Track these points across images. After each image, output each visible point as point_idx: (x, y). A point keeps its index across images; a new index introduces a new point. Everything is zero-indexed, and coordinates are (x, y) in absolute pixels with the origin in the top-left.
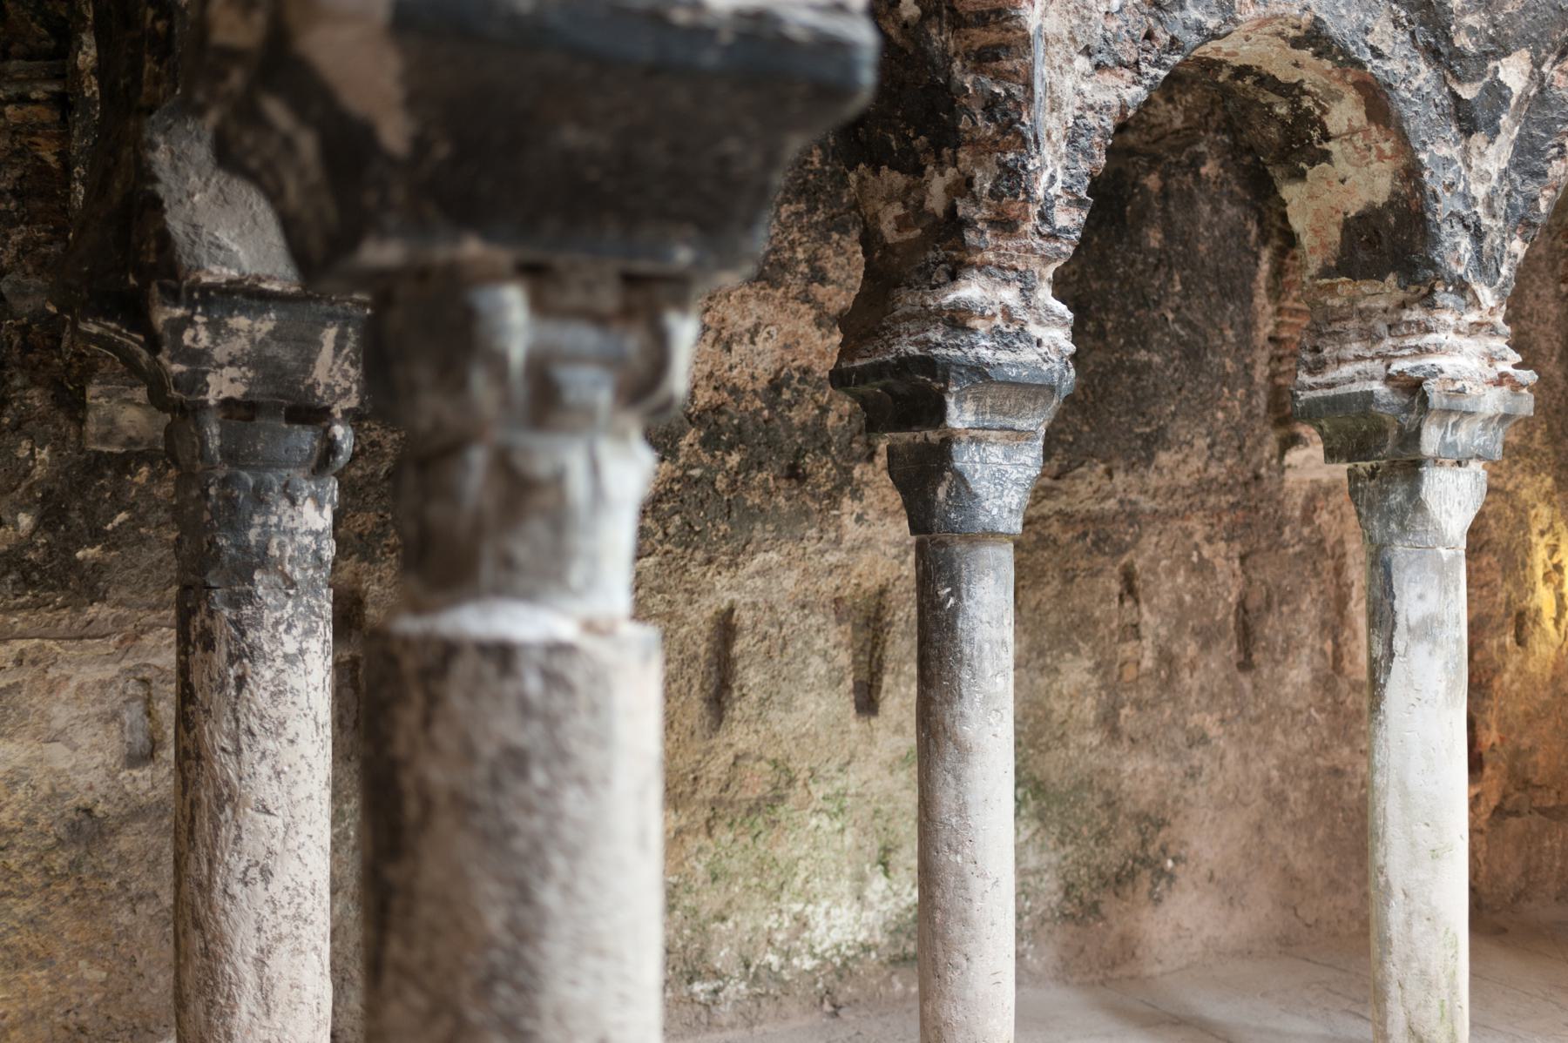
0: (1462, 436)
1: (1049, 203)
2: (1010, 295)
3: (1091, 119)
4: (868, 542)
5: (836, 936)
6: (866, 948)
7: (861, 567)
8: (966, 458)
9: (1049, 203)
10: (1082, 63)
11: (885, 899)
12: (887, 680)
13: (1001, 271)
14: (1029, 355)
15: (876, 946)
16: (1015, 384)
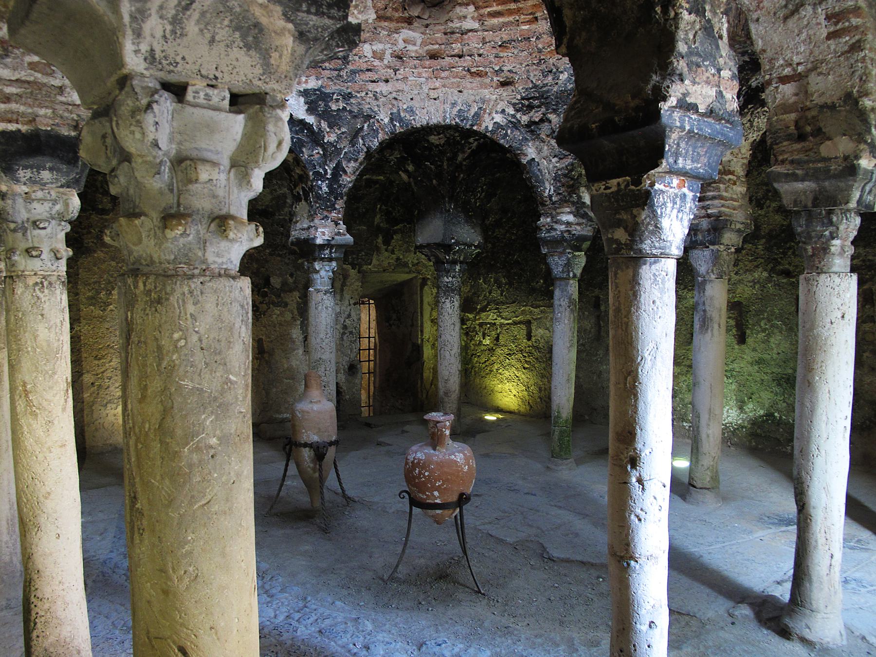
0: (700, 237)
1: (550, 196)
2: (549, 220)
3: (560, 173)
4: (740, 281)
5: (730, 419)
6: (743, 427)
7: (738, 291)
8: (550, 260)
9: (550, 196)
10: (554, 160)
11: (751, 412)
12: (748, 332)
13: (546, 215)
14: (553, 233)
15: (746, 427)
16: (549, 241)
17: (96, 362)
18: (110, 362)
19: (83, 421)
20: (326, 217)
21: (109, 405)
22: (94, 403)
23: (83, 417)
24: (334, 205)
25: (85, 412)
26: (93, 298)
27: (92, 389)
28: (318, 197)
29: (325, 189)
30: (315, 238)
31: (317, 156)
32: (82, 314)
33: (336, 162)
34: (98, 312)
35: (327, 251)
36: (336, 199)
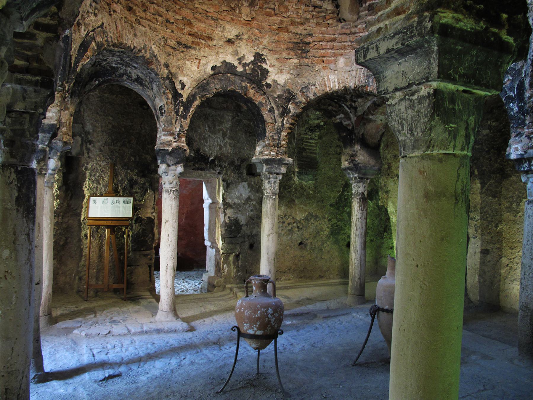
17: (511, 251)
18: (519, 252)
19: (500, 288)
20: (519, 135)
21: (515, 282)
22: (506, 278)
23: (500, 285)
24: (524, 120)
25: (501, 283)
26: (509, 207)
27: (506, 268)
28: (513, 118)
29: (516, 109)
30: (510, 154)
31: (508, 83)
32: (503, 217)
33: (517, 82)
34: (512, 218)
35: (526, 165)
36: (525, 116)
